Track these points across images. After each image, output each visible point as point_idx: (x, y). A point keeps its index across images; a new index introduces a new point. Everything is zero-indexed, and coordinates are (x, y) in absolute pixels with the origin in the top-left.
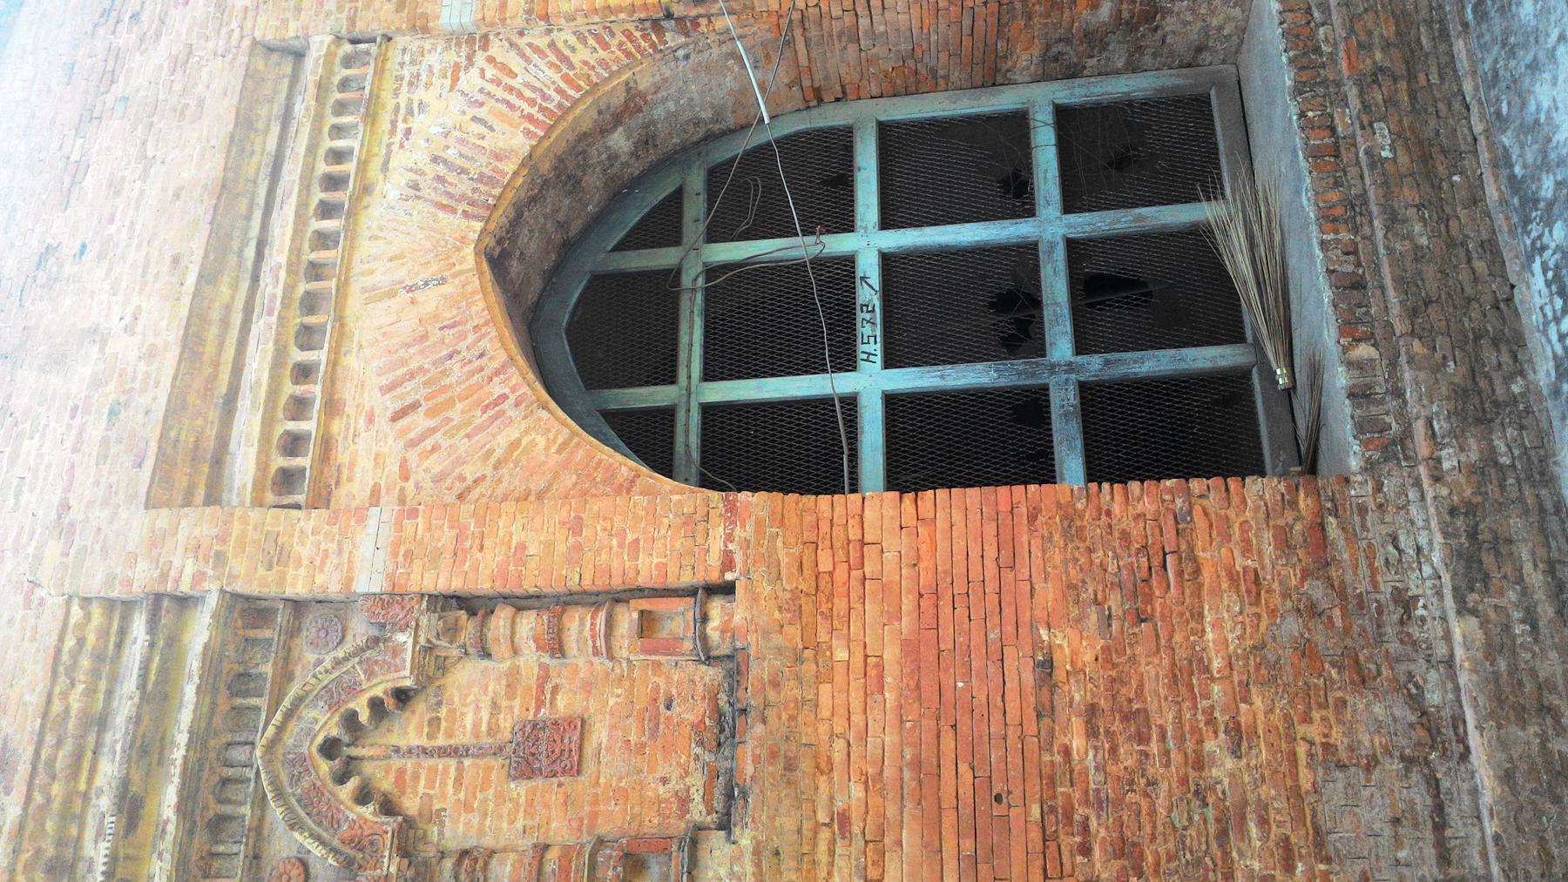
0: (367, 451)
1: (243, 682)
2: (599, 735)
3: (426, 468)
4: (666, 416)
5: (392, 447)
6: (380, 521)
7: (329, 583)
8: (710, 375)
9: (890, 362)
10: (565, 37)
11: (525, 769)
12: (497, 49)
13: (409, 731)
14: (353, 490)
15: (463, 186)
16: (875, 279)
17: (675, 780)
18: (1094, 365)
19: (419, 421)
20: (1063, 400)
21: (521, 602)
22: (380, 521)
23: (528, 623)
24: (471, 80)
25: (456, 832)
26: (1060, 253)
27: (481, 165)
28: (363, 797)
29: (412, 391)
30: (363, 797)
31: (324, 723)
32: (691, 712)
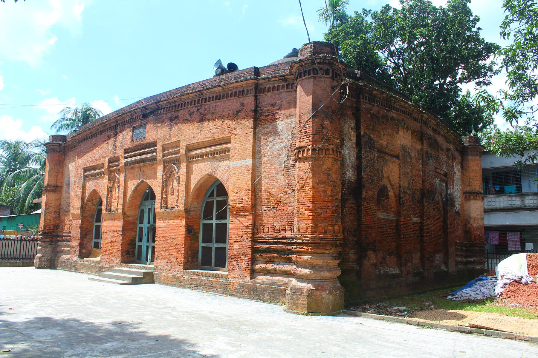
4: (213, 196)
8: (217, 201)
9: (216, 224)
15: (214, 170)
16: (224, 222)
18: (214, 249)
20: (210, 245)
24: (226, 168)
26: (224, 246)
28: (170, 175)
30: (170, 175)
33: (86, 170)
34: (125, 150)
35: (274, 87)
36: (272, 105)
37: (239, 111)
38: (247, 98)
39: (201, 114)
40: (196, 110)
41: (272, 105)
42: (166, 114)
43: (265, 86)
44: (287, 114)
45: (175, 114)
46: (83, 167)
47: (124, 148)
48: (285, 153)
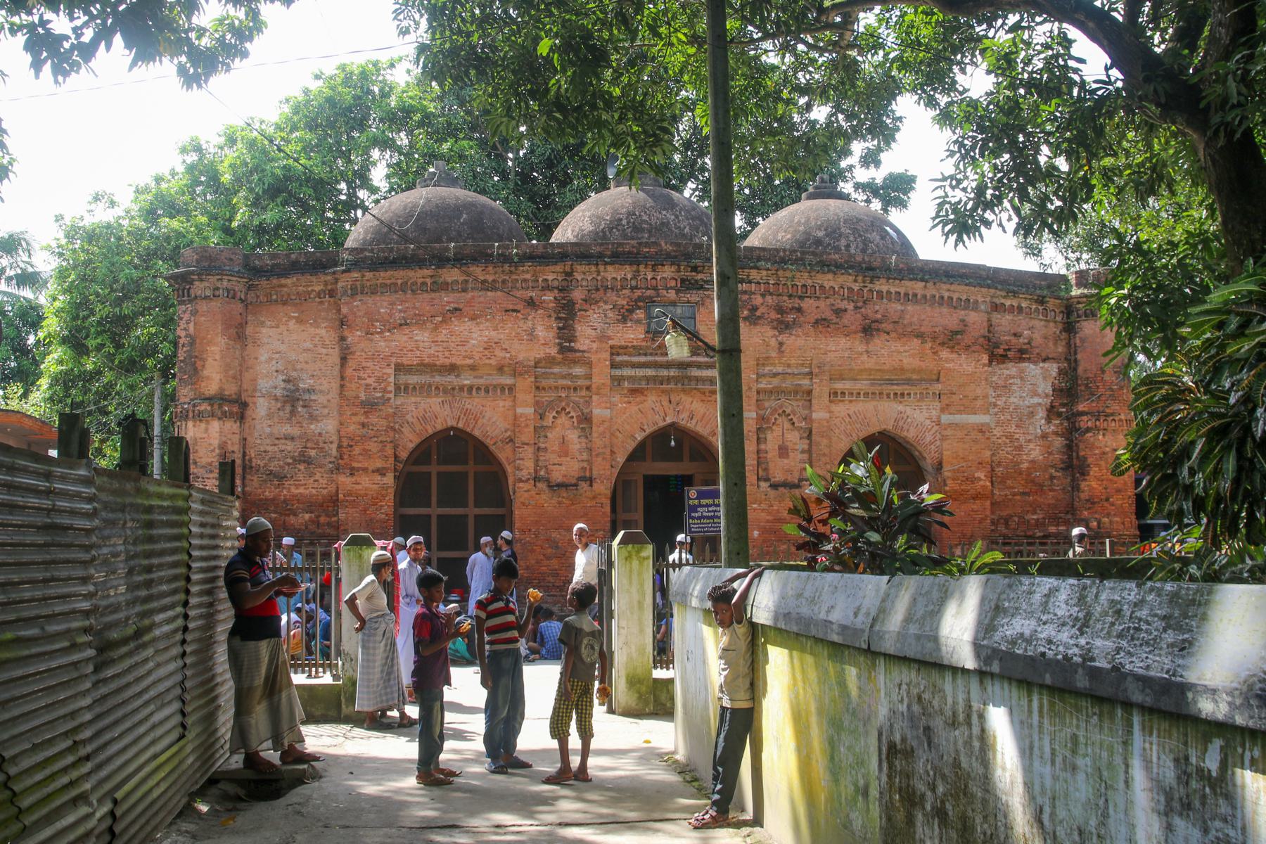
0: (841, 409)
1: (796, 393)
2: (786, 461)
3: (837, 421)
5: (842, 414)
6: (827, 415)
7: (815, 407)
10: (938, 443)
11: (780, 448)
12: (936, 428)
13: (787, 425)
14: (834, 407)
15: (901, 424)
17: (778, 477)
19: (847, 420)
21: (810, 445)
22: (827, 415)
23: (806, 447)
24: (928, 422)
25: (769, 436)
27: (906, 427)
29: (854, 417)
31: (788, 411)
32: (790, 479)
33: (399, 368)
34: (612, 347)
35: (1020, 309)
36: (1015, 335)
37: (957, 333)
38: (973, 314)
39: (865, 317)
40: (851, 307)
41: (1015, 335)
42: (763, 295)
43: (1003, 301)
44: (1044, 355)
45: (788, 303)
46: (394, 360)
47: (610, 342)
48: (1041, 414)
